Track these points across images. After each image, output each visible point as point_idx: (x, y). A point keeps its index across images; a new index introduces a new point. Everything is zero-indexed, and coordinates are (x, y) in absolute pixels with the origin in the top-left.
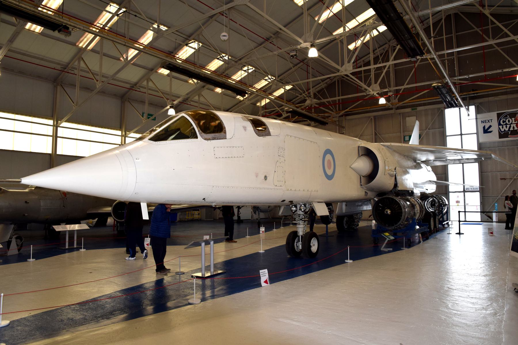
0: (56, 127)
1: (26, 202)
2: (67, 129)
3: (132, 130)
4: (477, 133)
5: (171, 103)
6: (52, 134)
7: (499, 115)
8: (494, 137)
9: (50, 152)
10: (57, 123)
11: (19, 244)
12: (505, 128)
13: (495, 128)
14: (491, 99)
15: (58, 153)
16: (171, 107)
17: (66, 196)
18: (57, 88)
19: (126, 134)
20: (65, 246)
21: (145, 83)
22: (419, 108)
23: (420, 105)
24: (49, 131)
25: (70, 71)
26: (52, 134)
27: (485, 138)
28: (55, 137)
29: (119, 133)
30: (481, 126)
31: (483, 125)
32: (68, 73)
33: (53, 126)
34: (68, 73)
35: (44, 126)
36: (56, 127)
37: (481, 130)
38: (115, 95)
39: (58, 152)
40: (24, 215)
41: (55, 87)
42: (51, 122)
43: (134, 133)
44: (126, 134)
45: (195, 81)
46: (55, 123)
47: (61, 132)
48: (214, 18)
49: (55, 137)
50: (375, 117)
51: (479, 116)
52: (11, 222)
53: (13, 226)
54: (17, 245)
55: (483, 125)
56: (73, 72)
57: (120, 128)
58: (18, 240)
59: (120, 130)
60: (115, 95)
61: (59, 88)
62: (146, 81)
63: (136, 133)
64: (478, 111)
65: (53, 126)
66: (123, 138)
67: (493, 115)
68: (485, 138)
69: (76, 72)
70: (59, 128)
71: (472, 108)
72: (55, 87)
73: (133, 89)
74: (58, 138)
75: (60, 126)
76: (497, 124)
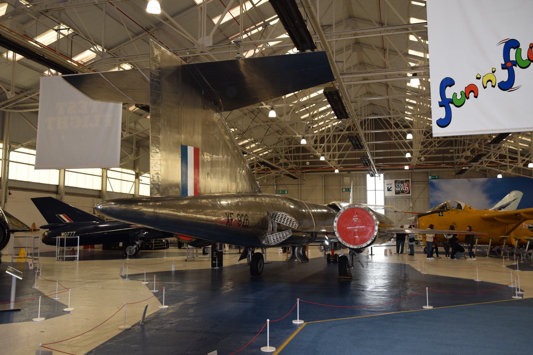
4: (384, 190)
7: (396, 181)
8: (392, 194)
12: (398, 189)
13: (393, 189)
14: (392, 171)
22: (352, 172)
23: (353, 171)
27: (388, 194)
30: (386, 187)
31: (387, 186)
37: (386, 189)
45: (53, 71)
48: (140, 36)
50: (324, 175)
51: (385, 181)
55: (387, 186)
64: (385, 178)
67: (393, 181)
68: (388, 194)
71: (382, 175)
76: (394, 186)
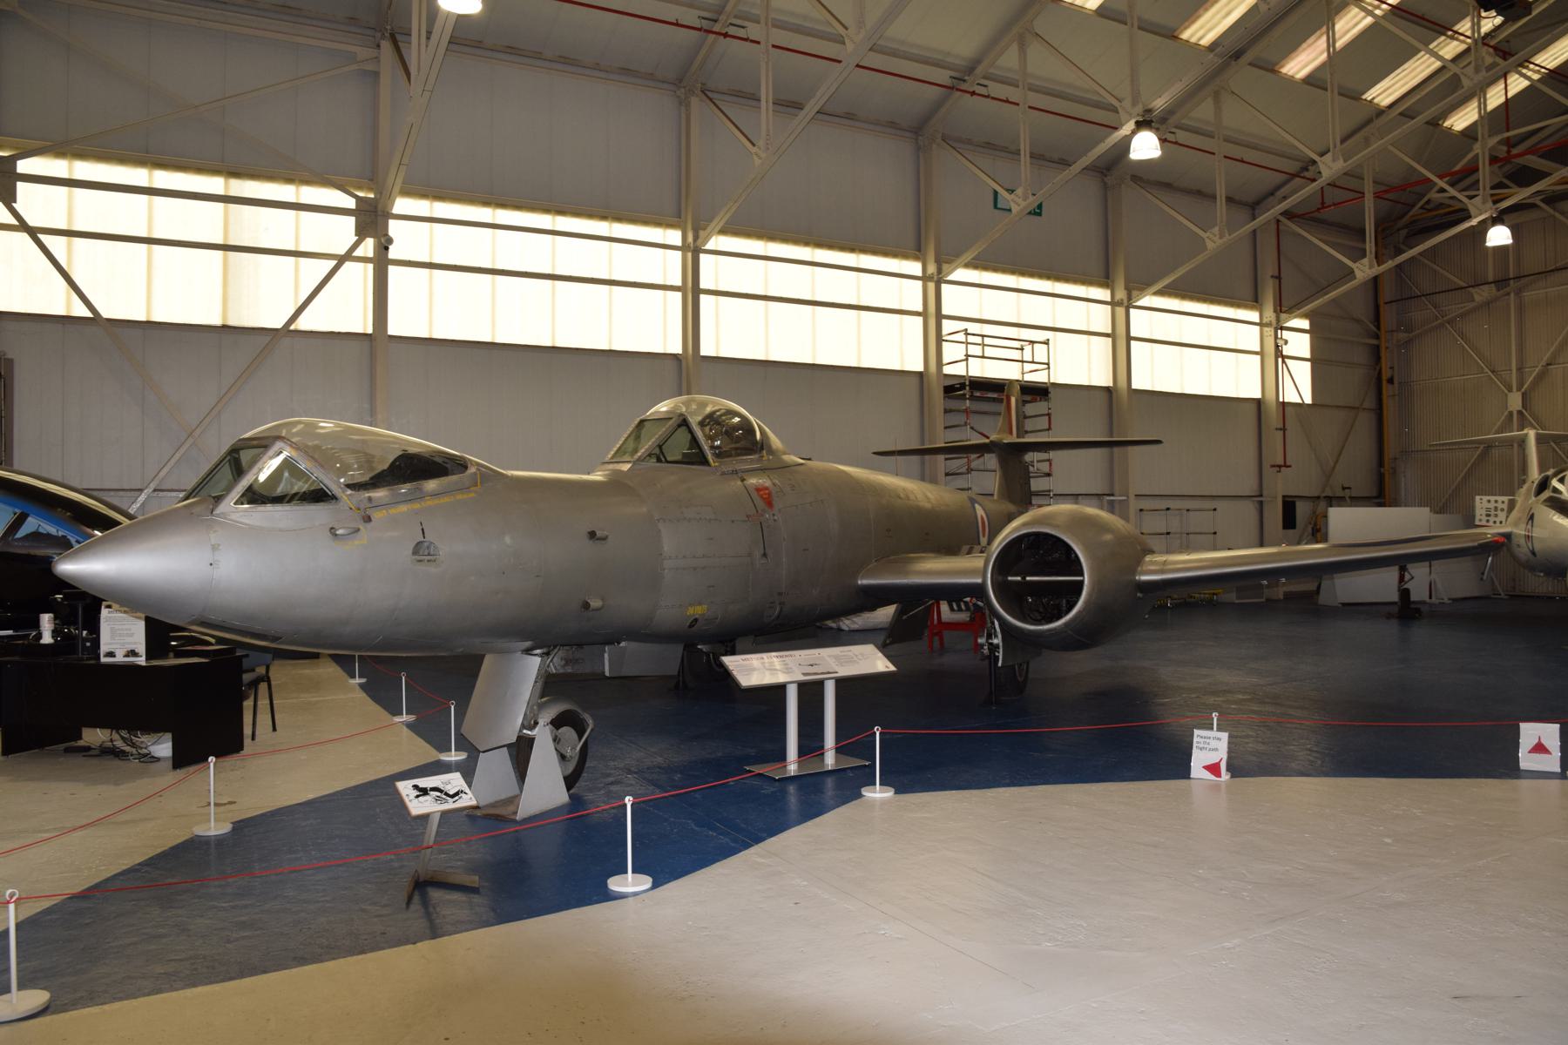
0: (693, 252)
1: (592, 535)
2: (733, 262)
3: (958, 255)
5: (1139, 109)
6: (679, 283)
9: (676, 347)
10: (696, 238)
11: (568, 752)
15: (703, 353)
16: (1140, 125)
17: (770, 504)
18: (688, 106)
19: (939, 271)
20: (781, 756)
21: (1009, 60)
24: (670, 267)
25: (732, 31)
26: (679, 283)
28: (692, 291)
29: (915, 268)
32: (726, 35)
33: (683, 248)
34: (726, 35)
35: (652, 253)
36: (693, 252)
38: (893, 125)
39: (706, 350)
40: (586, 606)
41: (683, 103)
42: (674, 236)
43: (967, 266)
44: (939, 271)
46: (690, 239)
47: (712, 271)
49: (692, 291)
52: (528, 644)
53: (534, 663)
54: (563, 757)
56: (741, 33)
57: (916, 252)
58: (567, 732)
59: (916, 258)
60: (893, 125)
61: (696, 102)
62: (1015, 47)
63: (976, 267)
65: (683, 248)
66: (931, 286)
69: (753, 31)
70: (702, 256)
72: (683, 103)
73: (964, 86)
74: (703, 297)
75: (708, 247)
